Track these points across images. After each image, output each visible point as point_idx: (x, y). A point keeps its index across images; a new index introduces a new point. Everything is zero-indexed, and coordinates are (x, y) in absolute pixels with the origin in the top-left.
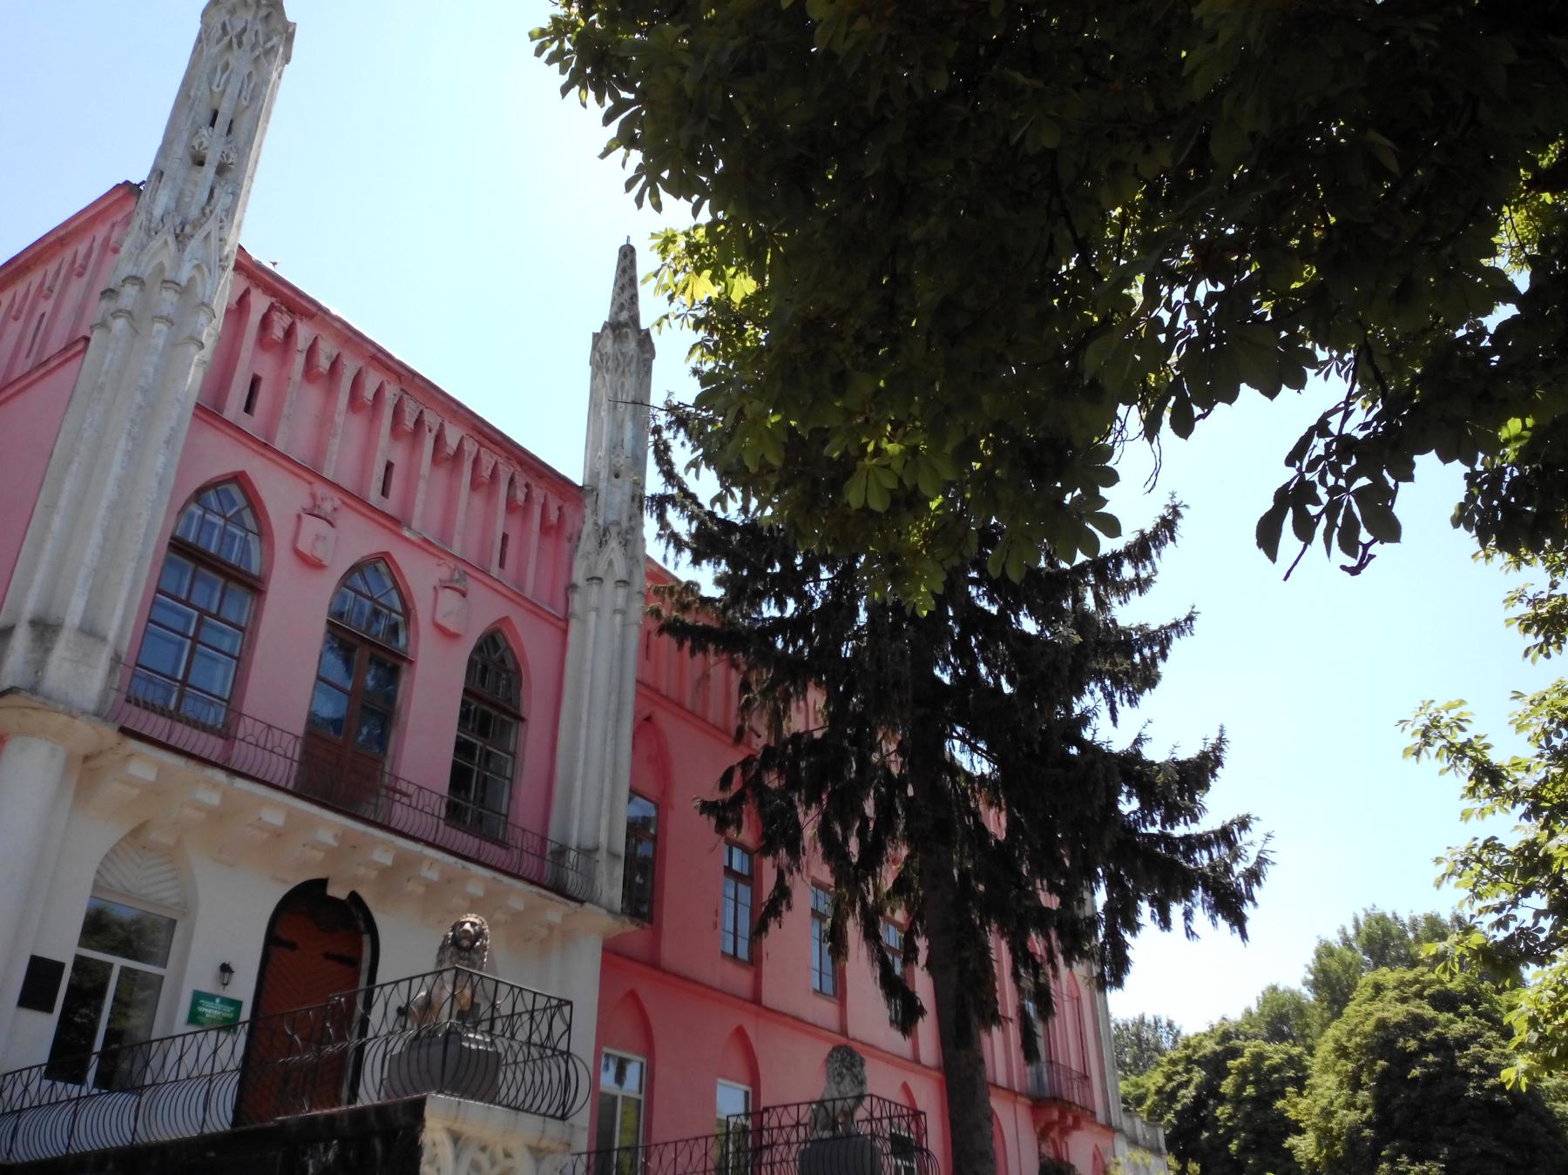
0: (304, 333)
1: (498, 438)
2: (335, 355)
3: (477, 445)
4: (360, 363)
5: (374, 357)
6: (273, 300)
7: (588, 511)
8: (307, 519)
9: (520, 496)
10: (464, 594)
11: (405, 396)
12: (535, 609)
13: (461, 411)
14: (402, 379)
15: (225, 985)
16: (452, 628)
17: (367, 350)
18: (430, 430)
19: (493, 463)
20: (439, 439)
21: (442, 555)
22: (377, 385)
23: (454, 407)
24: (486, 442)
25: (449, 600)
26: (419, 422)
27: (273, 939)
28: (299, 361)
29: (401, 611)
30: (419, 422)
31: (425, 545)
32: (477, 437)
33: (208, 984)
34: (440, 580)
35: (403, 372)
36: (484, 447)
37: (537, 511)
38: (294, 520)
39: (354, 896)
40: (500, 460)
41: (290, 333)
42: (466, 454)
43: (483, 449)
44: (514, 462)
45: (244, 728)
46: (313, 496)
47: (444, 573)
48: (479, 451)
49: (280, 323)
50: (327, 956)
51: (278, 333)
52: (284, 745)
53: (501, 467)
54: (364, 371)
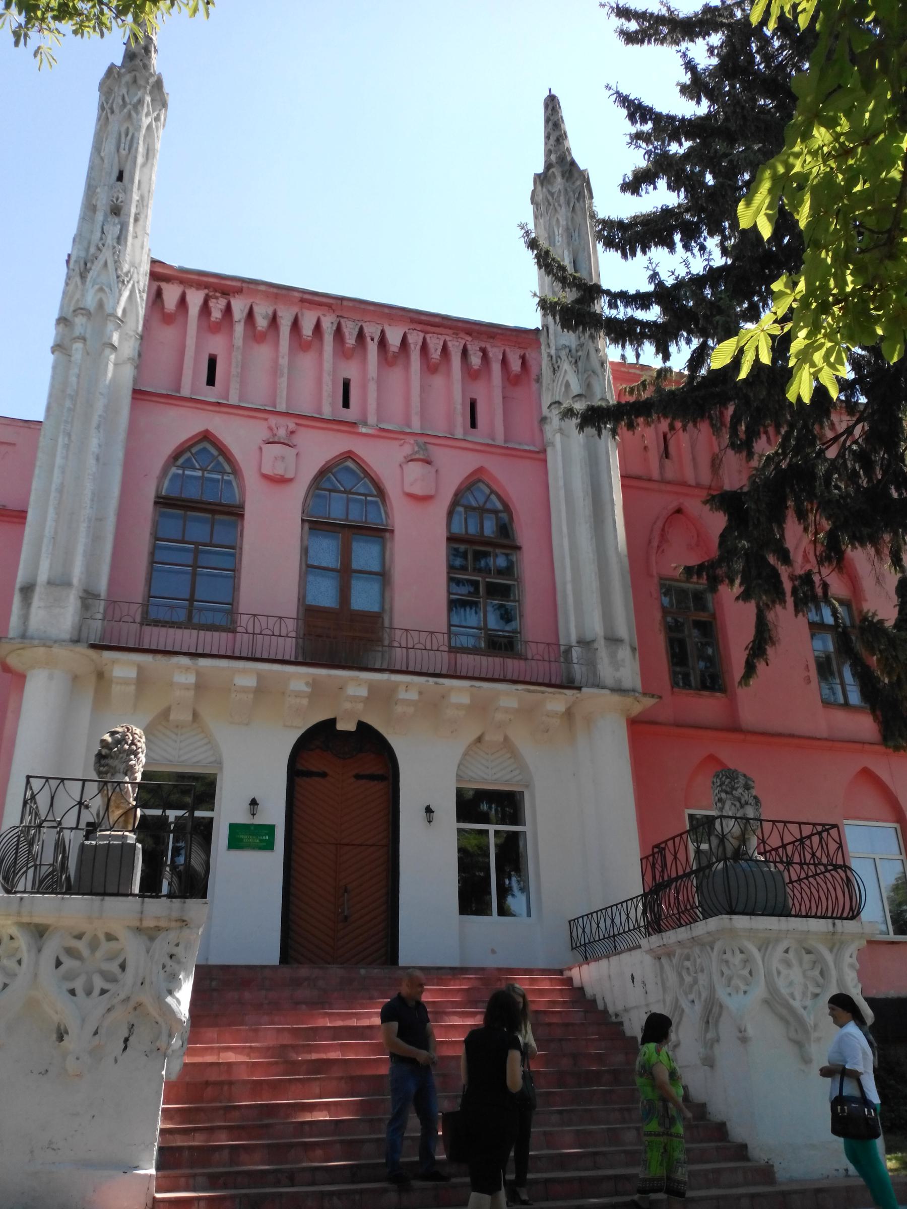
0: (239, 307)
1: (437, 320)
2: (270, 312)
3: (422, 335)
4: (294, 310)
5: (302, 301)
6: (206, 291)
7: (543, 347)
8: (266, 448)
9: (475, 360)
10: (428, 462)
11: (342, 321)
12: (509, 452)
13: (394, 311)
14: (333, 307)
15: (253, 815)
18: (372, 339)
19: (442, 344)
20: (383, 343)
21: (402, 437)
22: (314, 321)
23: (387, 311)
24: (429, 328)
25: (415, 470)
26: (361, 336)
27: (295, 771)
28: (239, 329)
29: (375, 493)
30: (361, 336)
31: (384, 434)
32: (419, 327)
33: (243, 818)
34: (405, 457)
35: (331, 301)
36: (426, 332)
37: (496, 367)
39: (361, 725)
40: (448, 338)
41: (228, 310)
42: (412, 346)
43: (428, 336)
44: (462, 335)
45: (244, 621)
46: (270, 429)
47: (407, 450)
48: (424, 340)
50: (358, 777)
51: (216, 314)
53: (450, 344)
54: (299, 315)
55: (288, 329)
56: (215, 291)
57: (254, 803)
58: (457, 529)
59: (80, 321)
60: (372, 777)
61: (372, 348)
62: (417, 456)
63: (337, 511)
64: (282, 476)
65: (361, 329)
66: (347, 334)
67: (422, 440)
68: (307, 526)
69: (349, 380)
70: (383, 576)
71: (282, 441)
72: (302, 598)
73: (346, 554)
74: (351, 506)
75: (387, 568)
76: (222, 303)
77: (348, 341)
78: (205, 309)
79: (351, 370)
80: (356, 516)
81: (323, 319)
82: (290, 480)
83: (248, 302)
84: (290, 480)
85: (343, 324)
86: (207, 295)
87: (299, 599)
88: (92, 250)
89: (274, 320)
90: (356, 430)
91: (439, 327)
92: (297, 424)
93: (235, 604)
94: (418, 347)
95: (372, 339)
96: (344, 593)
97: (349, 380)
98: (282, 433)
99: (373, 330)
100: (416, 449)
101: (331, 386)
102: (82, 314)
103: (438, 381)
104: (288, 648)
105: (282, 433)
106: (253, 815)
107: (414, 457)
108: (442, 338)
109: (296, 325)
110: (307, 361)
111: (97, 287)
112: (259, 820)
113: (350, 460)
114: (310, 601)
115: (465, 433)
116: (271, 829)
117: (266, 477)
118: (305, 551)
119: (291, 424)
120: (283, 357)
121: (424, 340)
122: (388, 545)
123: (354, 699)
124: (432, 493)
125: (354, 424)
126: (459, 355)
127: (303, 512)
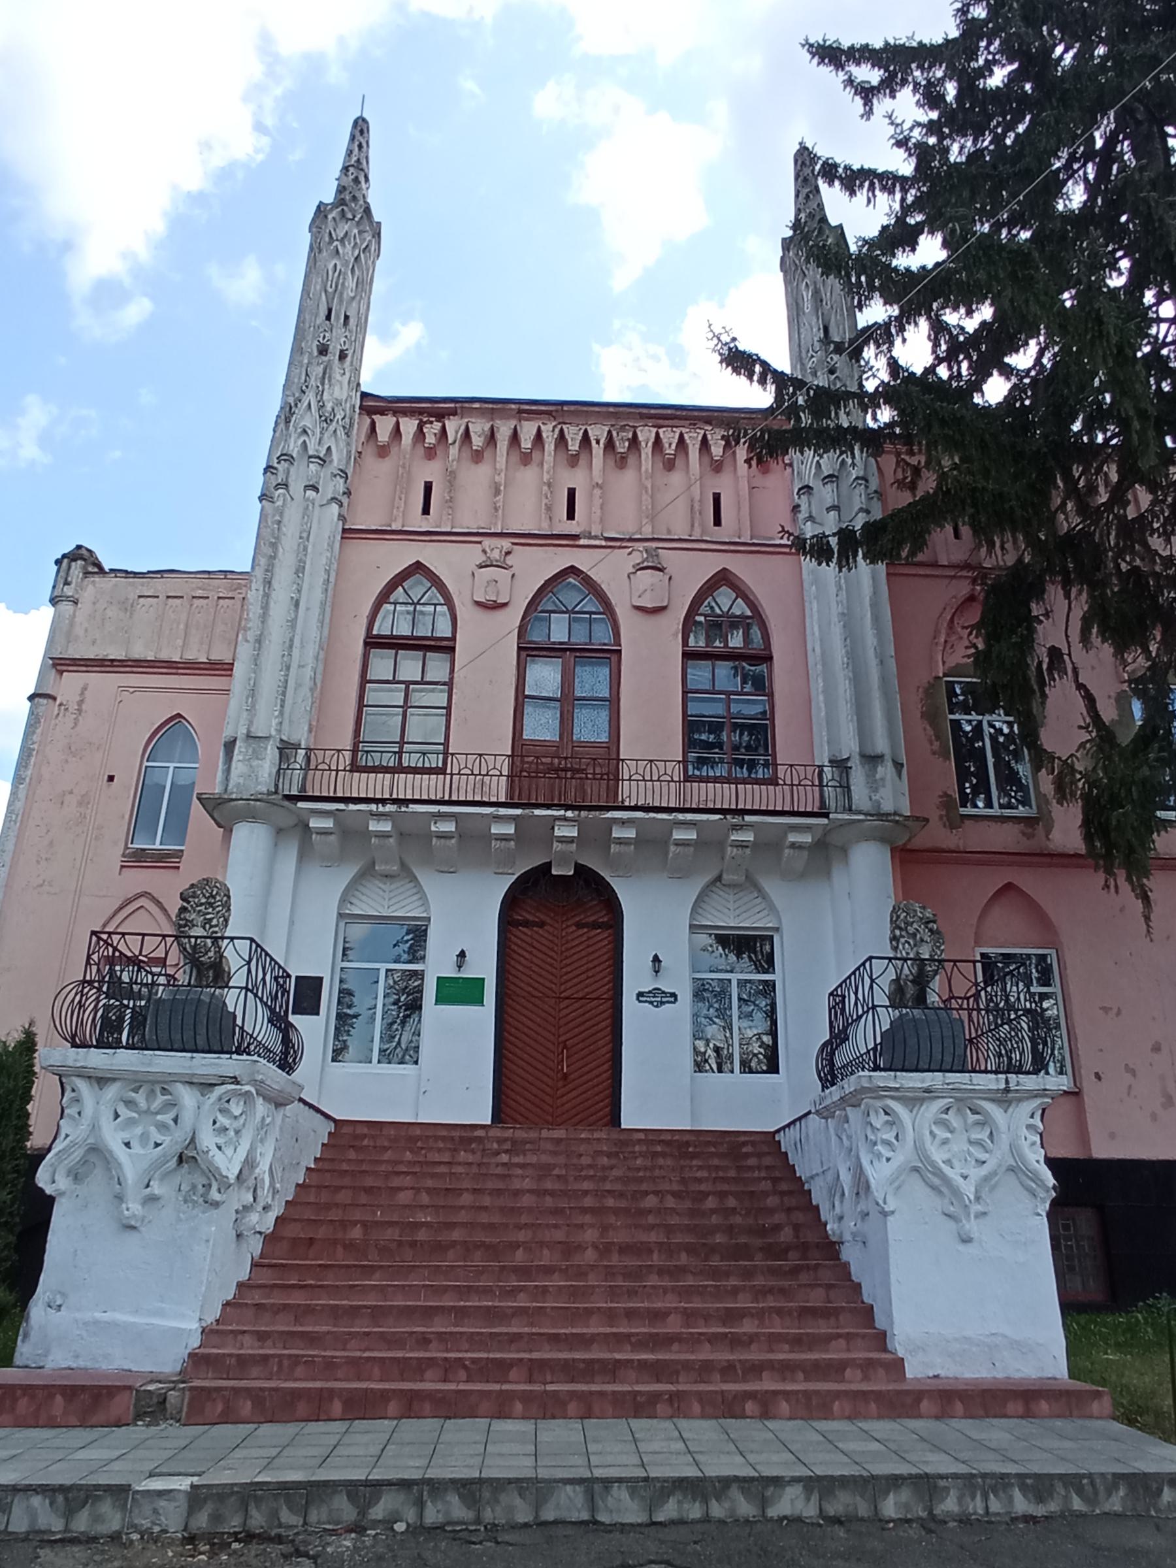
4: (512, 423)
15: (460, 967)
17: (511, 409)
21: (629, 544)
22: (534, 432)
25: (646, 578)
31: (614, 543)
33: (450, 972)
38: (470, 578)
46: (484, 551)
49: (432, 431)
51: (430, 439)
52: (327, 761)
57: (462, 954)
60: (595, 925)
63: (559, 631)
65: (586, 431)
73: (567, 681)
74: (575, 626)
80: (580, 637)
84: (505, 605)
89: (492, 438)
90: (577, 543)
96: (566, 723)
104: (499, 789)
105: (496, 555)
106: (460, 967)
109: (515, 437)
119: (506, 543)
123: (564, 840)
125: (576, 537)
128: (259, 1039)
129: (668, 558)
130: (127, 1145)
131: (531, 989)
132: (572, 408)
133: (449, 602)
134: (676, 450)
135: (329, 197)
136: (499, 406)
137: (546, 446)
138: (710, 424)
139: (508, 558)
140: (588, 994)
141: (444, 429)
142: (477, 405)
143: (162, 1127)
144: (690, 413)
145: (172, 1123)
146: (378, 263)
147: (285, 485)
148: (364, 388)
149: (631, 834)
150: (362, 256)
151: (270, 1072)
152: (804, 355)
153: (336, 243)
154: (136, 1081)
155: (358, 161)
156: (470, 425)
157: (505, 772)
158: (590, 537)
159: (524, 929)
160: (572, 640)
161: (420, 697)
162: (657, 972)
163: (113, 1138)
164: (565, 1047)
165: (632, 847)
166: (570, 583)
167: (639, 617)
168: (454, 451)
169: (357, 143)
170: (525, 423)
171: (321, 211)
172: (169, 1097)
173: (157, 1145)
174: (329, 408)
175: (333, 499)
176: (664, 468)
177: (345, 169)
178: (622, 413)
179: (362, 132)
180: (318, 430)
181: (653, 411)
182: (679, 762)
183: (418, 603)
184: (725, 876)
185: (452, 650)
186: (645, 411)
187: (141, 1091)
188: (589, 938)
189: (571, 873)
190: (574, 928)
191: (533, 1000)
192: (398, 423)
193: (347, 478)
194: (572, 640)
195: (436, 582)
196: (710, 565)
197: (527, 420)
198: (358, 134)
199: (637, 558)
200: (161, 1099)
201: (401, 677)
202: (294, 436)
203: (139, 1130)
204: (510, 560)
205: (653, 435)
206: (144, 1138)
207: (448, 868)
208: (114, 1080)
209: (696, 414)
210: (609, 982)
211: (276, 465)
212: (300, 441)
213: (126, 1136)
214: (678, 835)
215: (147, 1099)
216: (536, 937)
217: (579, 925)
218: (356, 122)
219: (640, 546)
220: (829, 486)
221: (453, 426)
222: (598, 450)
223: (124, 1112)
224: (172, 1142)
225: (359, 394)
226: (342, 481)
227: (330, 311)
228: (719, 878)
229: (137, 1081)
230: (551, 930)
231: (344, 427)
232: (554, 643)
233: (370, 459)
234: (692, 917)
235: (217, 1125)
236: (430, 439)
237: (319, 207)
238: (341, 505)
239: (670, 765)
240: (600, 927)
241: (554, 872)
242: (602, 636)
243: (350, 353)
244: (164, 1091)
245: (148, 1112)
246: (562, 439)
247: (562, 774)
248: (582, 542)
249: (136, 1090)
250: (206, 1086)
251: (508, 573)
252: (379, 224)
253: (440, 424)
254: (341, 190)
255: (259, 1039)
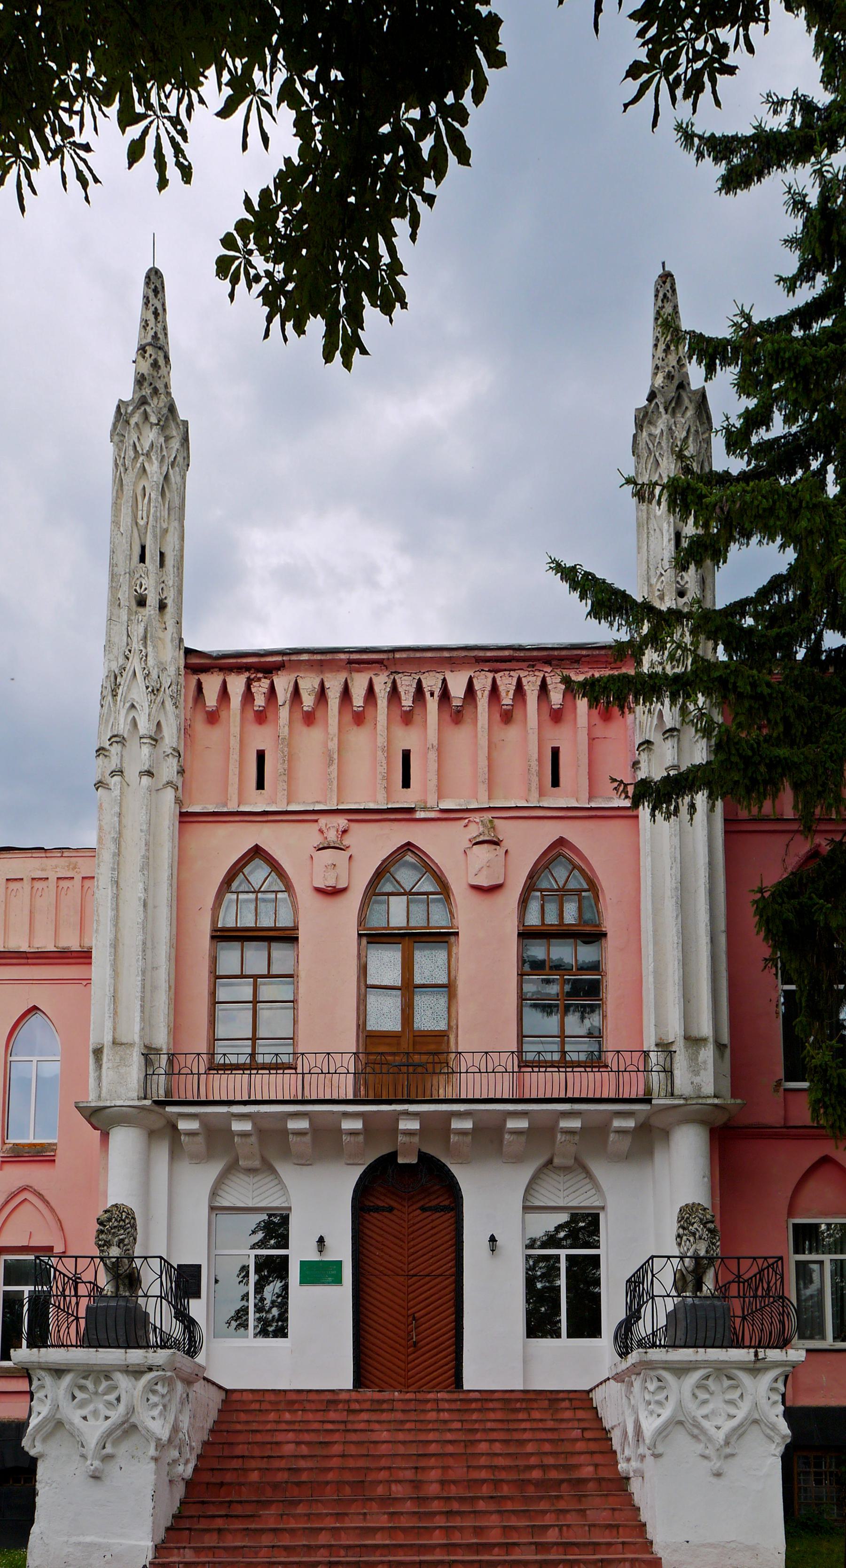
1: (506, 653)
2: (317, 685)
3: (490, 676)
6: (247, 674)
10: (496, 843)
11: (397, 677)
14: (385, 663)
16: (485, 883)
18: (432, 695)
19: (514, 682)
20: (445, 695)
25: (483, 853)
28: (284, 713)
31: (449, 815)
34: (470, 840)
36: (497, 671)
38: (309, 862)
40: (522, 674)
42: (479, 693)
43: (498, 676)
46: (321, 831)
48: (494, 681)
49: (260, 689)
51: (260, 701)
54: (349, 681)
55: (337, 701)
56: (258, 670)
58: (533, 919)
59: (115, 749)
61: (432, 704)
62: (482, 838)
64: (334, 887)
66: (402, 694)
67: (488, 816)
68: (364, 941)
69: (409, 751)
70: (449, 988)
71: (332, 845)
72: (361, 1024)
74: (413, 907)
75: (452, 977)
76: (265, 683)
77: (404, 703)
78: (248, 695)
79: (407, 738)
80: (418, 921)
81: (376, 680)
82: (344, 890)
83: (292, 677)
84: (344, 890)
85: (398, 681)
86: (248, 678)
87: (358, 1026)
88: (121, 660)
89: (322, 694)
91: (510, 661)
92: (349, 820)
93: (296, 1038)
94: (487, 693)
95: (432, 695)
97: (409, 751)
98: (332, 836)
99: (432, 682)
100: (481, 829)
101: (385, 766)
102: (117, 742)
103: (512, 733)
105: (332, 836)
107: (478, 840)
108: (515, 674)
109: (346, 693)
110: (359, 738)
111: (128, 705)
112: (329, 1256)
113: (409, 853)
114: (373, 1025)
115: (542, 794)
116: (339, 1264)
117: (319, 890)
118: (363, 970)
119: (341, 821)
120: (332, 740)
121: (494, 681)
122: (454, 950)
124: (501, 882)
125: (411, 810)
126: (536, 693)
127: (360, 924)
128: (174, 1336)
129: (506, 829)
130: (85, 1418)
131: (382, 1268)
132: (404, 655)
133: (289, 887)
134: (513, 700)
135: (127, 393)
136: (329, 657)
137: (379, 702)
138: (550, 665)
139: (346, 836)
140: (433, 1271)
141: (272, 688)
142: (305, 657)
143: (109, 1404)
144: (528, 654)
145: (116, 1402)
146: (189, 474)
147: (120, 772)
148: (188, 644)
149: (468, 1125)
150: (171, 471)
151: (181, 1358)
152: (652, 573)
153: (141, 458)
154: (85, 1371)
155: (155, 337)
156: (300, 682)
157: (352, 1070)
158: (425, 809)
159: (376, 1215)
160: (412, 924)
161: (269, 991)
162: (493, 1250)
163: (73, 1415)
164: (414, 1319)
165: (470, 1137)
166: (407, 862)
167: (475, 897)
168: (284, 713)
169: (152, 309)
170: (356, 676)
171: (121, 414)
172: (110, 1382)
173: (107, 1418)
174: (154, 675)
175: (168, 783)
176: (502, 720)
177: (142, 349)
178: (458, 658)
179: (156, 292)
180: (146, 704)
181: (489, 654)
182: (513, 1052)
183: (259, 891)
184: (556, 1161)
185: (296, 939)
186: (481, 654)
187: (90, 1378)
188: (433, 1221)
189: (415, 1161)
190: (418, 1211)
191: (386, 1278)
192: (224, 684)
193: (180, 755)
194: (410, 925)
195: (275, 867)
196: (549, 832)
197: (358, 671)
198: (151, 295)
199: (474, 831)
200: (104, 1384)
201: (247, 972)
202: (123, 712)
203: (91, 1407)
204: (346, 842)
205: (490, 681)
206: (95, 1413)
207: (304, 1161)
208: (69, 1371)
209: (535, 653)
210: (452, 1260)
211: (107, 747)
212: (131, 717)
213: (84, 1412)
214: (511, 1124)
215: (95, 1384)
216: (385, 1220)
217: (423, 1209)
218: (148, 277)
219: (476, 817)
220: (669, 743)
221: (283, 683)
222: (432, 704)
223: (80, 1395)
224: (117, 1414)
225: (182, 652)
226: (176, 760)
227: (143, 548)
228: (550, 1162)
229: (88, 1372)
230: (399, 1214)
231: (172, 697)
232: (394, 929)
233: (200, 726)
234: (525, 1199)
235: (150, 1402)
236: (260, 701)
237: (118, 407)
238: (177, 789)
239: (504, 1056)
240: (442, 1210)
241: (400, 1161)
242: (439, 919)
243: (169, 602)
244: (108, 1378)
245: (96, 1393)
246: (394, 694)
247: (404, 1069)
248: (420, 815)
249: (85, 1378)
250: (136, 1372)
251: (345, 855)
252: (185, 423)
253: (268, 682)
254: (140, 381)
255: (174, 1336)
